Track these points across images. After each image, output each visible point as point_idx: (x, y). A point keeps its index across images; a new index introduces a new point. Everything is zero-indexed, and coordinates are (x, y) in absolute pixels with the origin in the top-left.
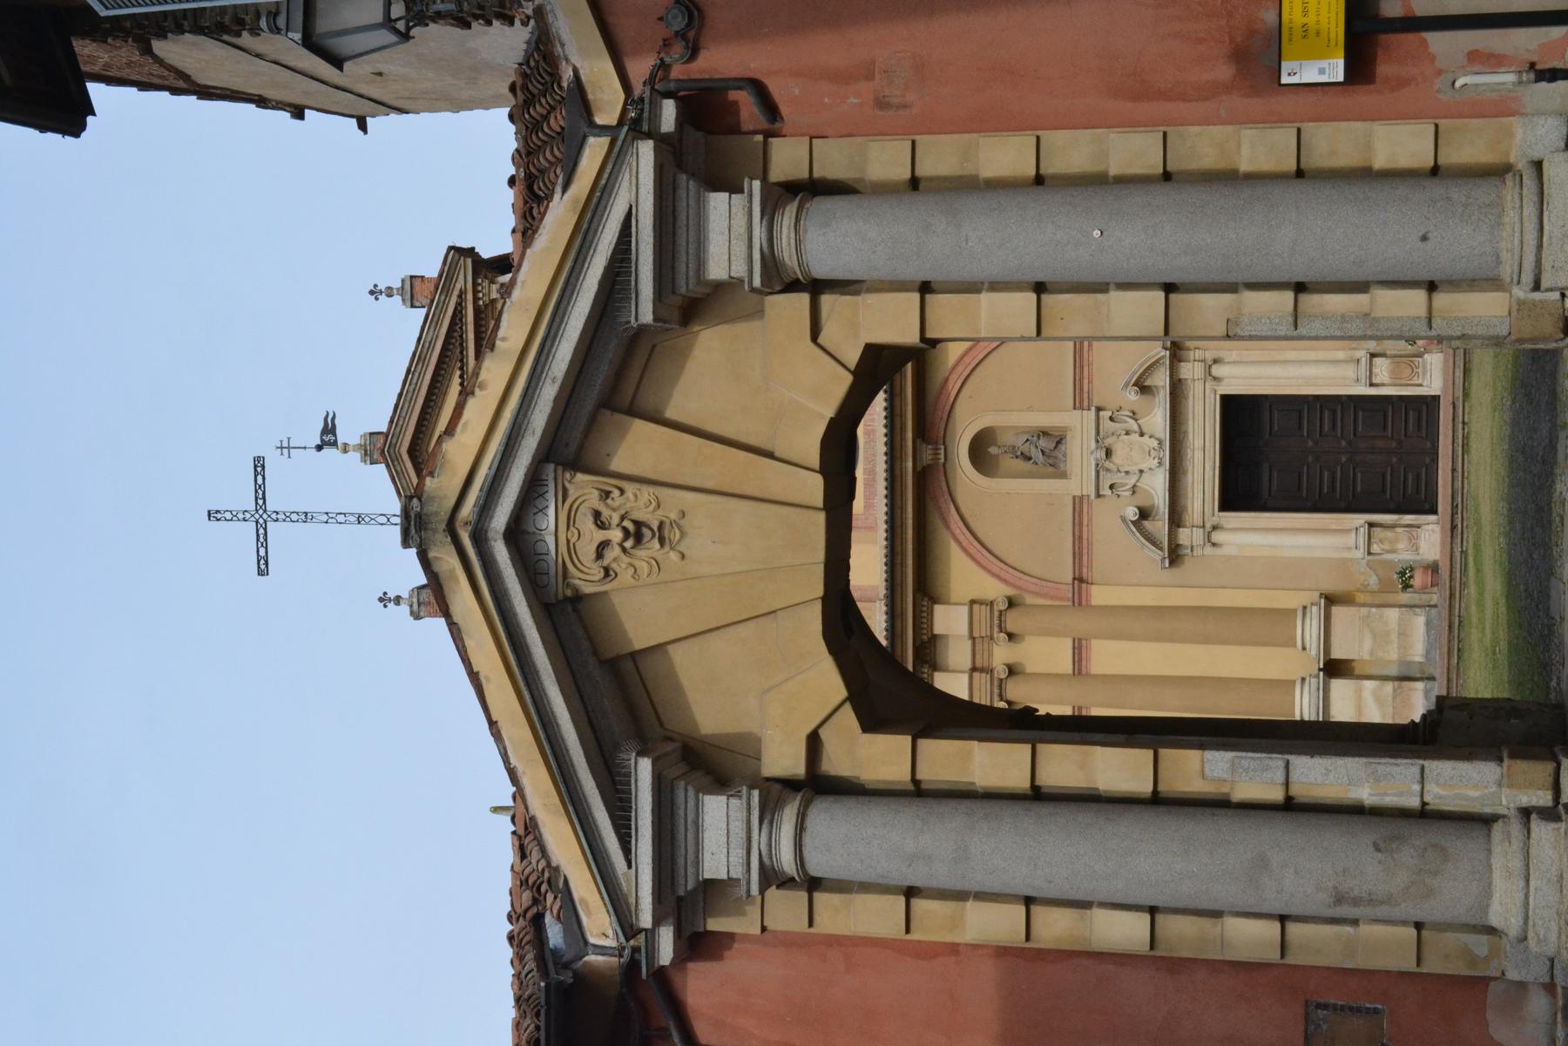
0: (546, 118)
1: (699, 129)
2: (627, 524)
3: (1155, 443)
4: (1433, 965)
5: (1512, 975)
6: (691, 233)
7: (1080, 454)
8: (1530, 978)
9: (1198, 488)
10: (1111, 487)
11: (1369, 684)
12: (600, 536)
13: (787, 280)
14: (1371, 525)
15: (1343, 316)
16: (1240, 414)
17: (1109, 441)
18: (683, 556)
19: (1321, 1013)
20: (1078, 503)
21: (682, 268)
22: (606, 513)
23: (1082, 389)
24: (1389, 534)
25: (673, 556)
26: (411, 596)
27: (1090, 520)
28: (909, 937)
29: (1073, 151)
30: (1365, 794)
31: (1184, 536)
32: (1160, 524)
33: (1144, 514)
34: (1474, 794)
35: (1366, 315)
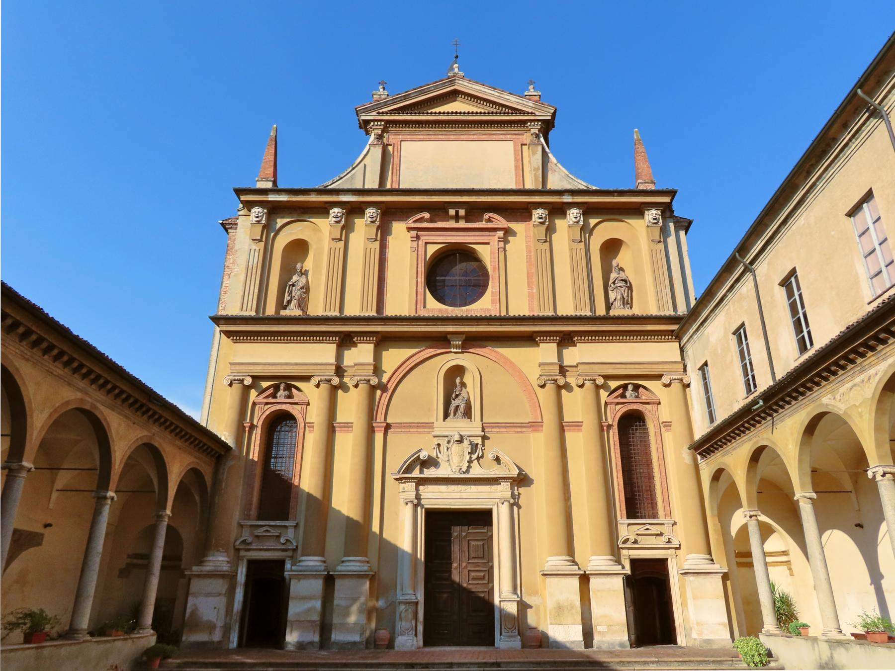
3: (464, 469)
7: (457, 426)
11: (318, 604)
14: (417, 603)
23: (493, 427)
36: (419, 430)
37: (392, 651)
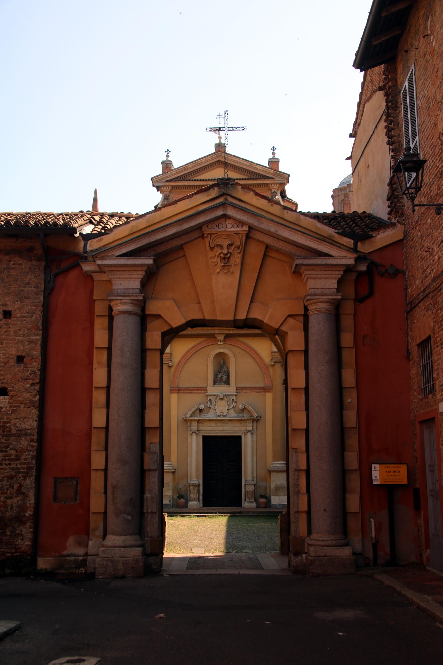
0: (357, 226)
1: (357, 277)
2: (229, 255)
3: (225, 414)
4: (92, 518)
5: (90, 543)
6: (324, 276)
7: (221, 389)
8: (89, 548)
9: (210, 429)
12: (225, 246)
13: (308, 307)
15: (299, 485)
16: (235, 442)
17: (226, 399)
18: (218, 273)
19: (75, 483)
20: (205, 389)
21: (313, 272)
22: (233, 248)
23: (242, 390)
24: (196, 492)
25: (218, 270)
26: (169, 161)
27: (199, 393)
28: (94, 349)
29: (351, 398)
30: (148, 495)
31: (195, 424)
32: (199, 416)
33: (201, 411)
34: (148, 529)
35: (299, 492)
36: (198, 391)
37: (187, 508)
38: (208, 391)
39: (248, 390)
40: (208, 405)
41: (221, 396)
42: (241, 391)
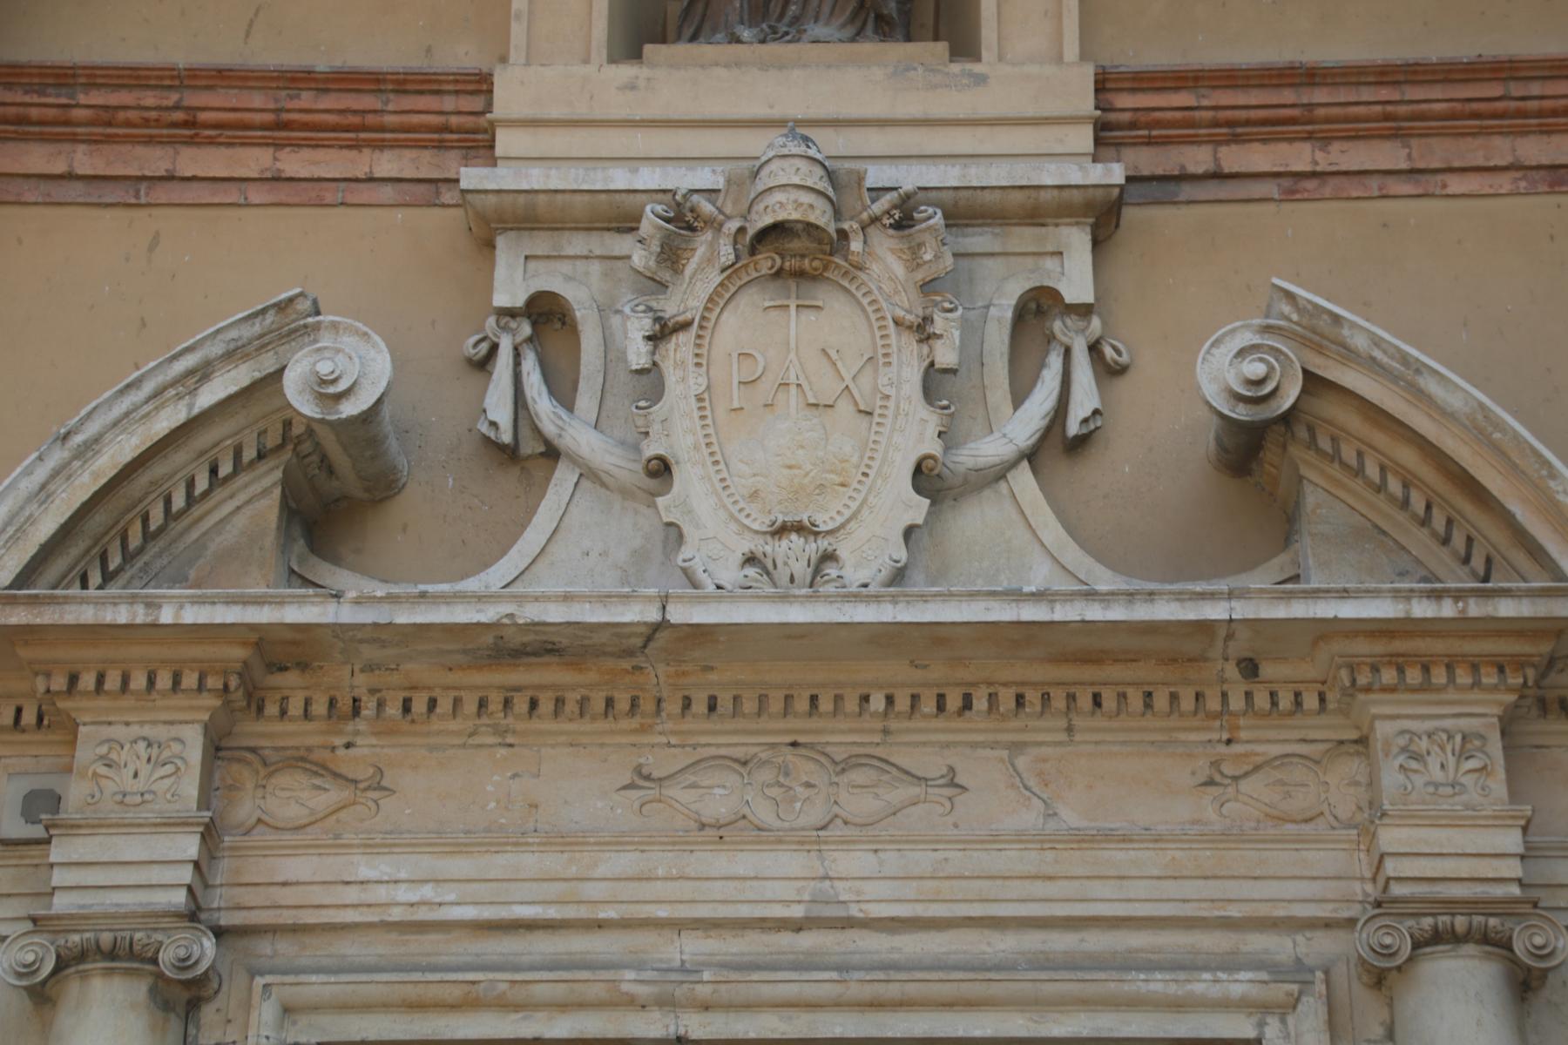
9: (522, 883)
10: (546, 315)
17: (886, 263)
23: (1235, 130)
31: (145, 760)
36: (295, 163)
38: (506, 142)
39: (1356, 130)
40: (499, 407)
41: (790, 195)
42: (1198, 159)
